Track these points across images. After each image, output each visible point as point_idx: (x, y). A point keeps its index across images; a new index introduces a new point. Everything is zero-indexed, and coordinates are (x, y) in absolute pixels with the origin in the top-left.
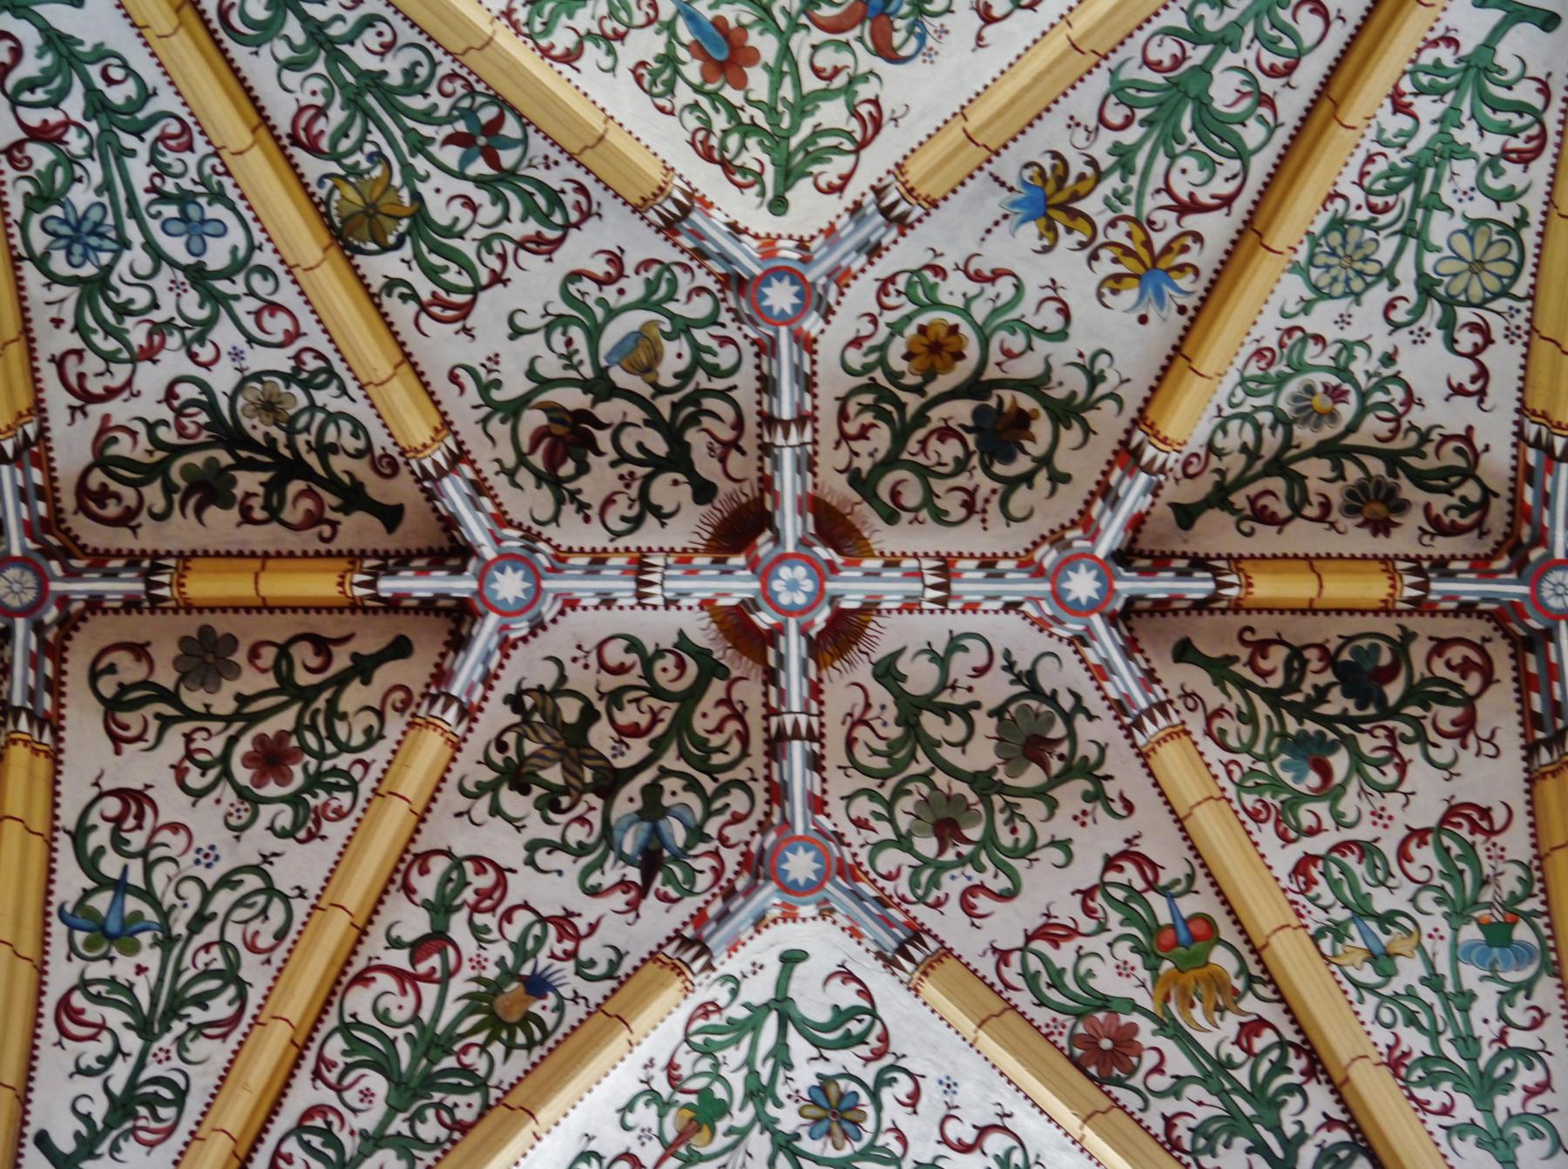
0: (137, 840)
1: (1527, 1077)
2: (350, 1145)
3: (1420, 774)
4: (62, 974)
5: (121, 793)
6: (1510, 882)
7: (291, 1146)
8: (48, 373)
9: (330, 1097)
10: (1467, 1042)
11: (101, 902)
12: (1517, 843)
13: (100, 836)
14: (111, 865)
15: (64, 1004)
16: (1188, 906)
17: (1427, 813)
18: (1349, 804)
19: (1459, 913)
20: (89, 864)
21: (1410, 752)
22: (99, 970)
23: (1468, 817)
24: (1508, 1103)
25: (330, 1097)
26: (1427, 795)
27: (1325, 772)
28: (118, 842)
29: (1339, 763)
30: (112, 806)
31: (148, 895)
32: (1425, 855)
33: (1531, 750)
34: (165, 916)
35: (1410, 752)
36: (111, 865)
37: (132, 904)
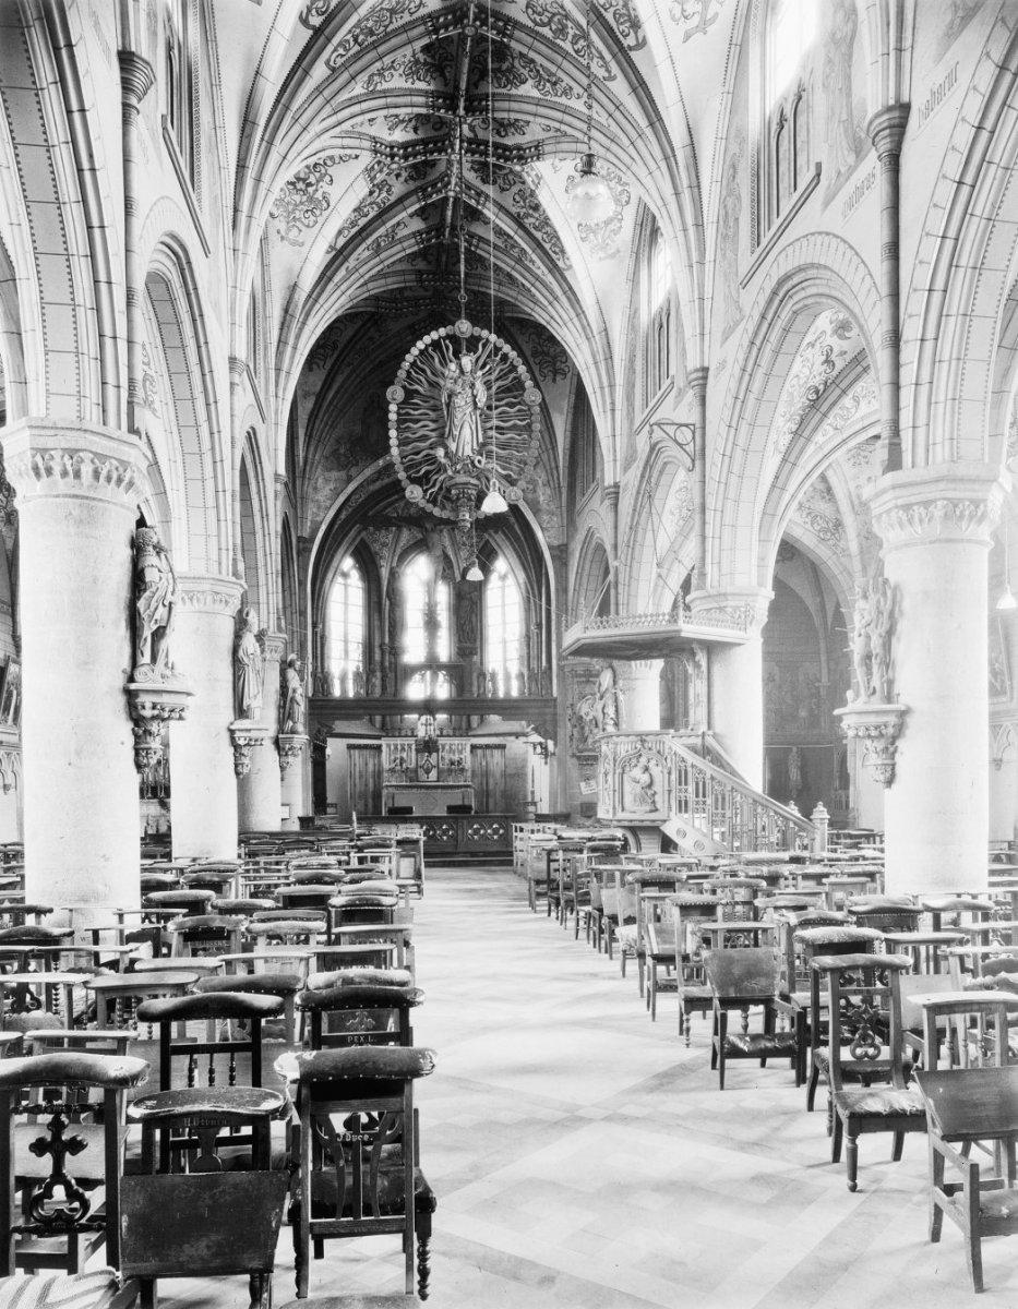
0: (539, 9)
2: (624, 11)
4: (567, 46)
5: (527, 7)
7: (621, 28)
8: (415, 16)
9: (612, 9)
11: (554, 27)
13: (538, 19)
14: (546, 20)
15: (577, 52)
20: (543, 25)
22: (570, 37)
25: (612, 9)
28: (539, 14)
30: (530, 11)
31: (554, 15)
34: (559, 14)
36: (546, 20)
37: (556, 19)
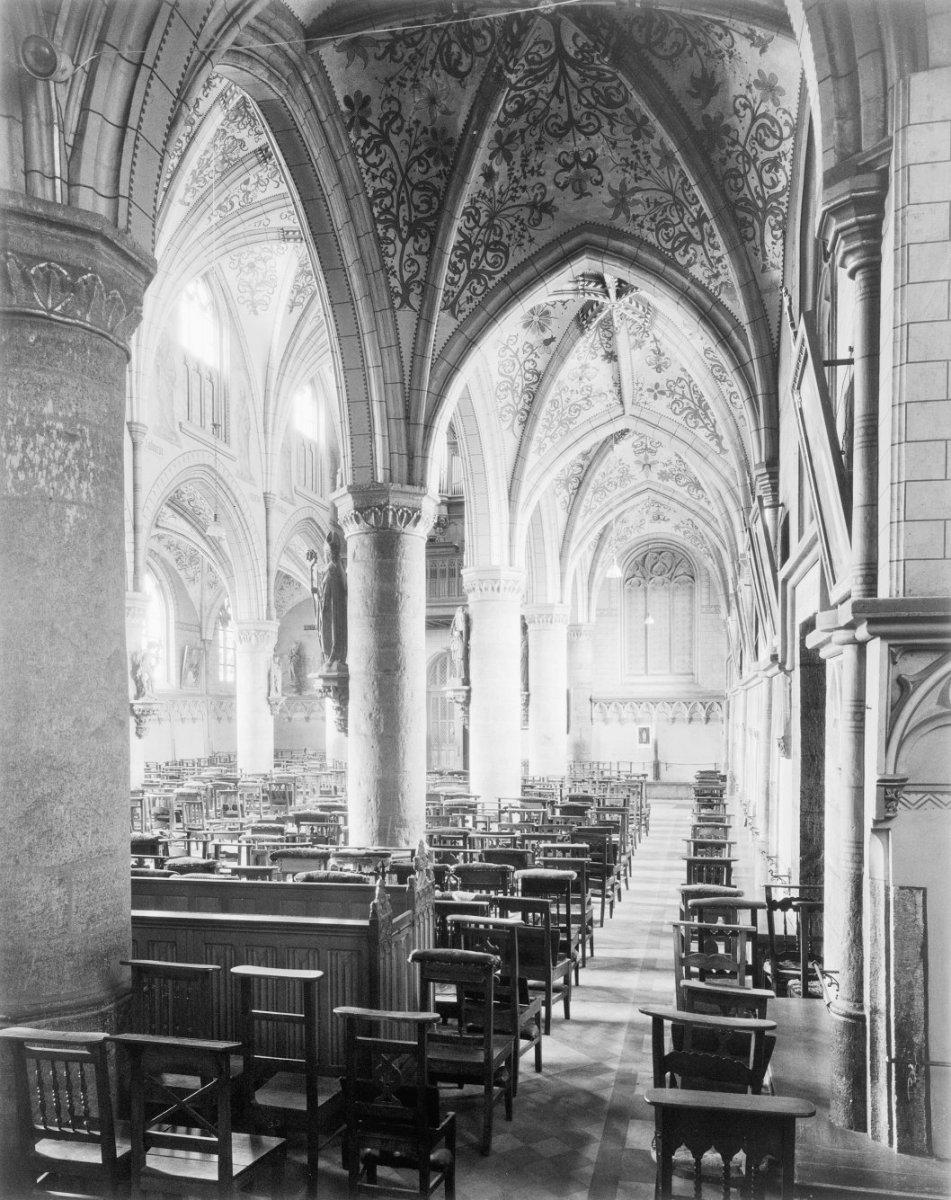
1: (202, 184)
3: (245, 132)
6: (234, 157)
10: (201, 172)
12: (242, 154)
16: (195, 117)
17: (238, 137)
18: (232, 125)
19: (223, 153)
21: (249, 127)
23: (242, 143)
24: (195, 185)
26: (243, 134)
27: (236, 117)
29: (239, 118)
32: (230, 141)
33: (260, 149)
35: (249, 127)
